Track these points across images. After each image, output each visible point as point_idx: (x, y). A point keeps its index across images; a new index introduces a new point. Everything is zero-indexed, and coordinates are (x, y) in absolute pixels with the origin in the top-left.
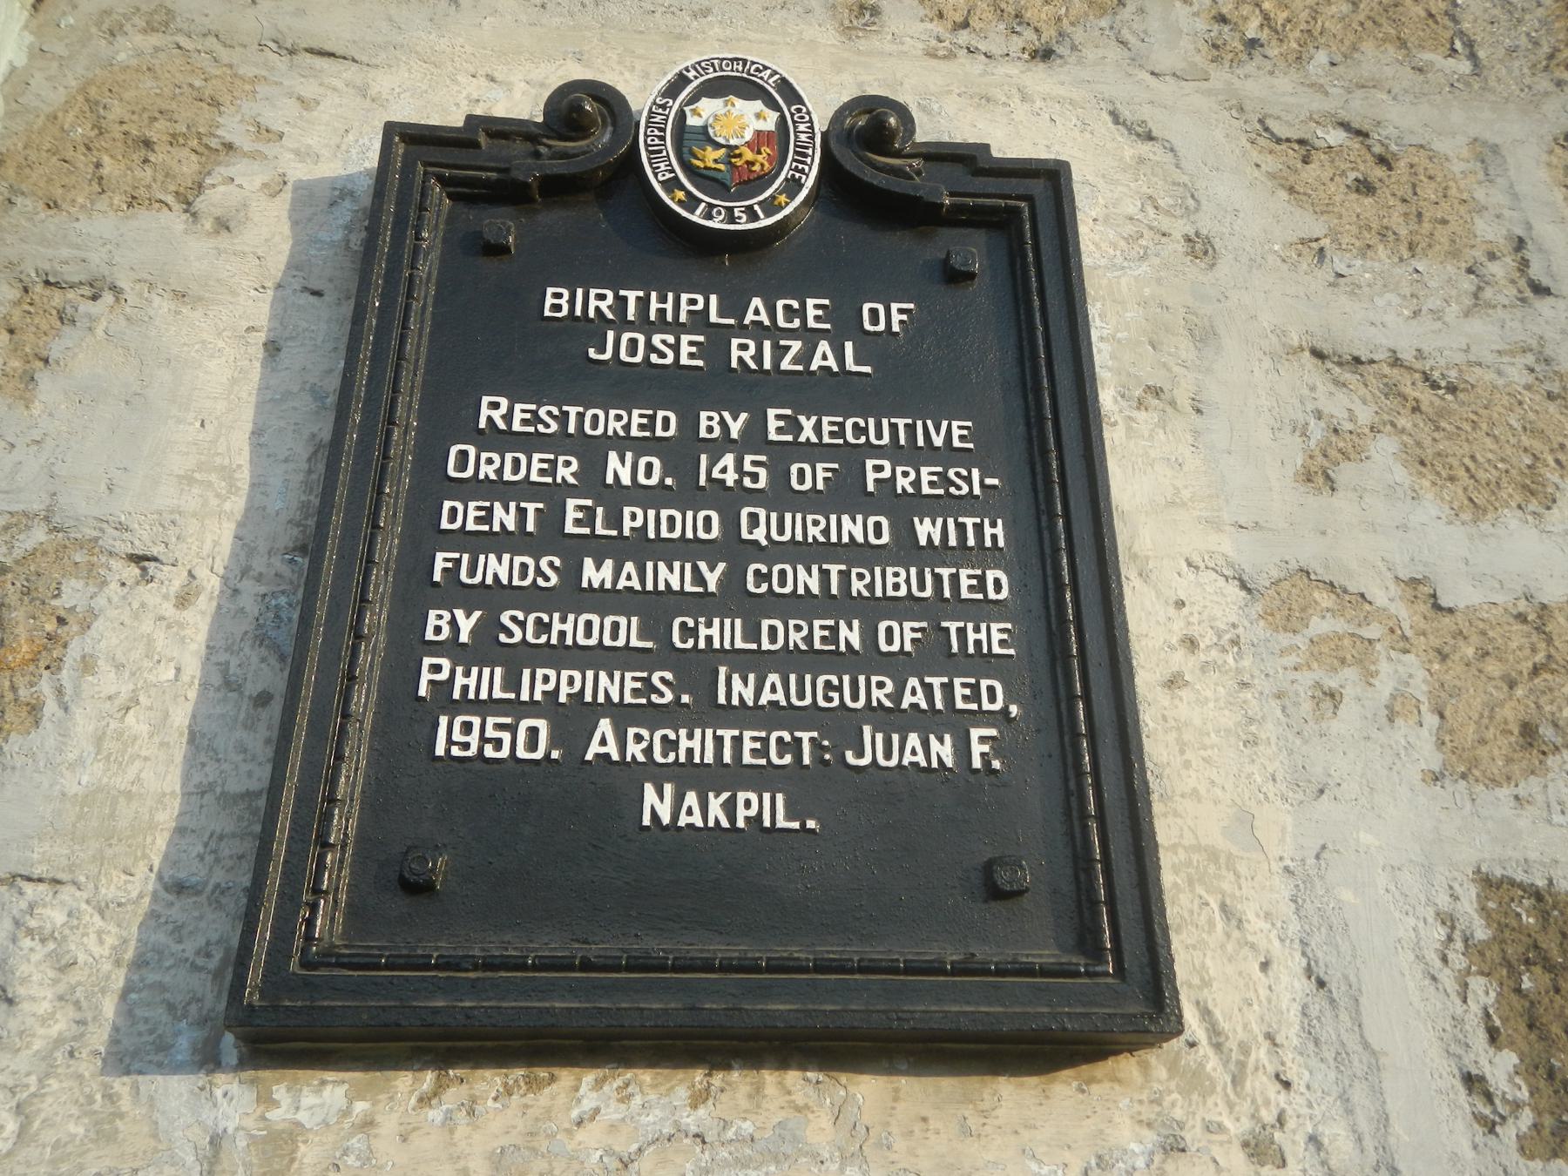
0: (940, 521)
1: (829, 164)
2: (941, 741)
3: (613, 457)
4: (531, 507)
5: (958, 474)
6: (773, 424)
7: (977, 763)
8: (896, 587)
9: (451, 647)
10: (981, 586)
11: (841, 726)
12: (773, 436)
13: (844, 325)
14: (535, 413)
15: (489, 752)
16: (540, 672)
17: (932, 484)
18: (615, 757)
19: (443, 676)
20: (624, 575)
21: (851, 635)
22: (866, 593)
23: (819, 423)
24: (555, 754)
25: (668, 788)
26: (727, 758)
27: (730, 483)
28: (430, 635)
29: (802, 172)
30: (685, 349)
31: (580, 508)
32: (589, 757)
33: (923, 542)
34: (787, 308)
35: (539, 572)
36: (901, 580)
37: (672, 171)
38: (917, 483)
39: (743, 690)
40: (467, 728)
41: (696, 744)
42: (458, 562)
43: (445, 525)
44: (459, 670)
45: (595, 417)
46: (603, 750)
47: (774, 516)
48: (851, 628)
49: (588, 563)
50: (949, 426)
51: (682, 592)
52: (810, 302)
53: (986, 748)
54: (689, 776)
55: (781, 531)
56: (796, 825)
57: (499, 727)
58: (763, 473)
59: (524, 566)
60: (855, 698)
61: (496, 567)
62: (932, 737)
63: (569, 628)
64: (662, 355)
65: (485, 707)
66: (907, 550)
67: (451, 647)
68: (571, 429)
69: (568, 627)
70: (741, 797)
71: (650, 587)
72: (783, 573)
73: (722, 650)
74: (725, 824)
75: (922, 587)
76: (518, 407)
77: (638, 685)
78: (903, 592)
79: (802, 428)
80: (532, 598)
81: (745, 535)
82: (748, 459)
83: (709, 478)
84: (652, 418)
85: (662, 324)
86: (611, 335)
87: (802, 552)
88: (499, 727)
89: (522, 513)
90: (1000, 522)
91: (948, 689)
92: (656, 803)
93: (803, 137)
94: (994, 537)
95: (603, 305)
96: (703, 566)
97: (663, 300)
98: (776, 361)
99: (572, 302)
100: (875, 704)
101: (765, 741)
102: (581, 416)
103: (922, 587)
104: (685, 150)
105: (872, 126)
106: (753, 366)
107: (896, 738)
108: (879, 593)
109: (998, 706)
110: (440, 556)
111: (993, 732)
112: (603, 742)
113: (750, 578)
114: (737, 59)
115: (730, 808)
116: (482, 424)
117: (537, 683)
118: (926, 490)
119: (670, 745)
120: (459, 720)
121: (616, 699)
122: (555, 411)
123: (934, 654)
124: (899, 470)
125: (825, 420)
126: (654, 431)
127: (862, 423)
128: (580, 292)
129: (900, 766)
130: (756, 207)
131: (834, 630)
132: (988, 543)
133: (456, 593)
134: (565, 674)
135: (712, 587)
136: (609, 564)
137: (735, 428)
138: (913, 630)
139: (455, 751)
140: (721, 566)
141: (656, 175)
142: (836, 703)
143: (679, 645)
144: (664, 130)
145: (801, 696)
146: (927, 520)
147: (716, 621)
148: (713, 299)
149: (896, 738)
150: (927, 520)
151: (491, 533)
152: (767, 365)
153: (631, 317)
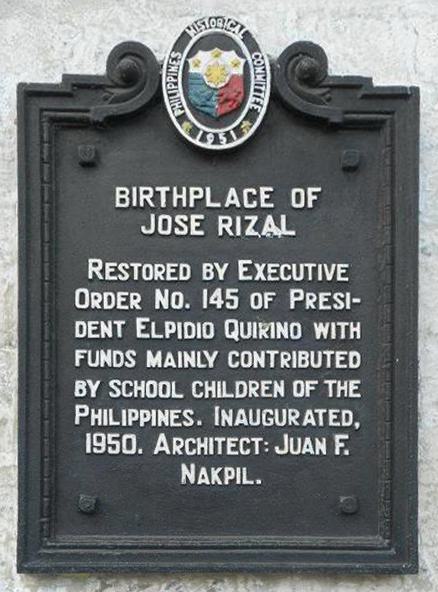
0: (327, 325)
1: (275, 97)
2: (321, 441)
3: (158, 292)
4: (119, 324)
5: (339, 297)
6: (242, 270)
7: (337, 452)
8: (303, 362)
9: (87, 399)
10: (346, 361)
11: (273, 435)
12: (242, 277)
13: (280, 204)
15: (110, 451)
16: (131, 411)
17: (325, 303)
18: (168, 452)
19: (86, 414)
20: (167, 360)
21: (279, 389)
22: (288, 366)
23: (266, 268)
25: (193, 466)
26: (220, 452)
28: (77, 394)
29: (258, 104)
30: (194, 224)
31: (143, 323)
32: (156, 452)
33: (318, 337)
34: (250, 194)
35: (126, 359)
36: (306, 358)
37: (182, 109)
38: (316, 303)
39: (227, 418)
41: (205, 446)
42: (86, 355)
43: (78, 335)
44: (93, 411)
45: (148, 269)
47: (242, 324)
49: (149, 353)
50: (336, 268)
51: (196, 368)
52: (263, 190)
53: (342, 445)
54: (204, 461)
55: (246, 332)
56: (252, 483)
57: (114, 439)
58: (236, 299)
59: (118, 356)
60: (281, 420)
61: (105, 358)
62: (317, 440)
63: (143, 388)
64: (181, 229)
65: (107, 429)
66: (308, 342)
67: (87, 399)
68: (136, 278)
69: (142, 388)
70: (227, 470)
71: (180, 366)
72: (246, 356)
73: (216, 399)
74: (220, 483)
75: (316, 361)
76: (108, 265)
77: (177, 417)
78: (306, 365)
80: (122, 373)
81: (228, 336)
82: (228, 291)
83: (209, 305)
84: (177, 268)
85: (180, 209)
86: (153, 216)
87: (255, 344)
88: (114, 439)
89: (115, 327)
90: (359, 324)
91: (326, 415)
92: (187, 473)
93: (259, 77)
94: (355, 333)
96: (206, 353)
97: (180, 192)
98: (243, 231)
99: (130, 196)
101: (237, 443)
102: (140, 269)
103: (316, 361)
105: (303, 65)
106: (231, 234)
107: (299, 440)
108: (294, 366)
109: (349, 424)
110: (78, 352)
111: (346, 437)
112: (162, 445)
113: (230, 358)
115: (221, 475)
116: (90, 277)
117: (129, 416)
118: (322, 307)
119: (192, 446)
120: (95, 436)
121: (167, 424)
122: (127, 267)
123: (319, 398)
128: (134, 189)
129: (301, 454)
130: (232, 132)
131: (271, 386)
132: (352, 337)
133: (85, 372)
134: (142, 412)
136: (159, 353)
137: (221, 273)
138: (311, 385)
139: (95, 451)
142: (272, 423)
143: (196, 396)
144: (176, 77)
145: (255, 420)
146: (321, 324)
148: (208, 190)
149: (299, 440)
150: (321, 324)
151: (100, 339)
152: (238, 233)
153: (163, 205)
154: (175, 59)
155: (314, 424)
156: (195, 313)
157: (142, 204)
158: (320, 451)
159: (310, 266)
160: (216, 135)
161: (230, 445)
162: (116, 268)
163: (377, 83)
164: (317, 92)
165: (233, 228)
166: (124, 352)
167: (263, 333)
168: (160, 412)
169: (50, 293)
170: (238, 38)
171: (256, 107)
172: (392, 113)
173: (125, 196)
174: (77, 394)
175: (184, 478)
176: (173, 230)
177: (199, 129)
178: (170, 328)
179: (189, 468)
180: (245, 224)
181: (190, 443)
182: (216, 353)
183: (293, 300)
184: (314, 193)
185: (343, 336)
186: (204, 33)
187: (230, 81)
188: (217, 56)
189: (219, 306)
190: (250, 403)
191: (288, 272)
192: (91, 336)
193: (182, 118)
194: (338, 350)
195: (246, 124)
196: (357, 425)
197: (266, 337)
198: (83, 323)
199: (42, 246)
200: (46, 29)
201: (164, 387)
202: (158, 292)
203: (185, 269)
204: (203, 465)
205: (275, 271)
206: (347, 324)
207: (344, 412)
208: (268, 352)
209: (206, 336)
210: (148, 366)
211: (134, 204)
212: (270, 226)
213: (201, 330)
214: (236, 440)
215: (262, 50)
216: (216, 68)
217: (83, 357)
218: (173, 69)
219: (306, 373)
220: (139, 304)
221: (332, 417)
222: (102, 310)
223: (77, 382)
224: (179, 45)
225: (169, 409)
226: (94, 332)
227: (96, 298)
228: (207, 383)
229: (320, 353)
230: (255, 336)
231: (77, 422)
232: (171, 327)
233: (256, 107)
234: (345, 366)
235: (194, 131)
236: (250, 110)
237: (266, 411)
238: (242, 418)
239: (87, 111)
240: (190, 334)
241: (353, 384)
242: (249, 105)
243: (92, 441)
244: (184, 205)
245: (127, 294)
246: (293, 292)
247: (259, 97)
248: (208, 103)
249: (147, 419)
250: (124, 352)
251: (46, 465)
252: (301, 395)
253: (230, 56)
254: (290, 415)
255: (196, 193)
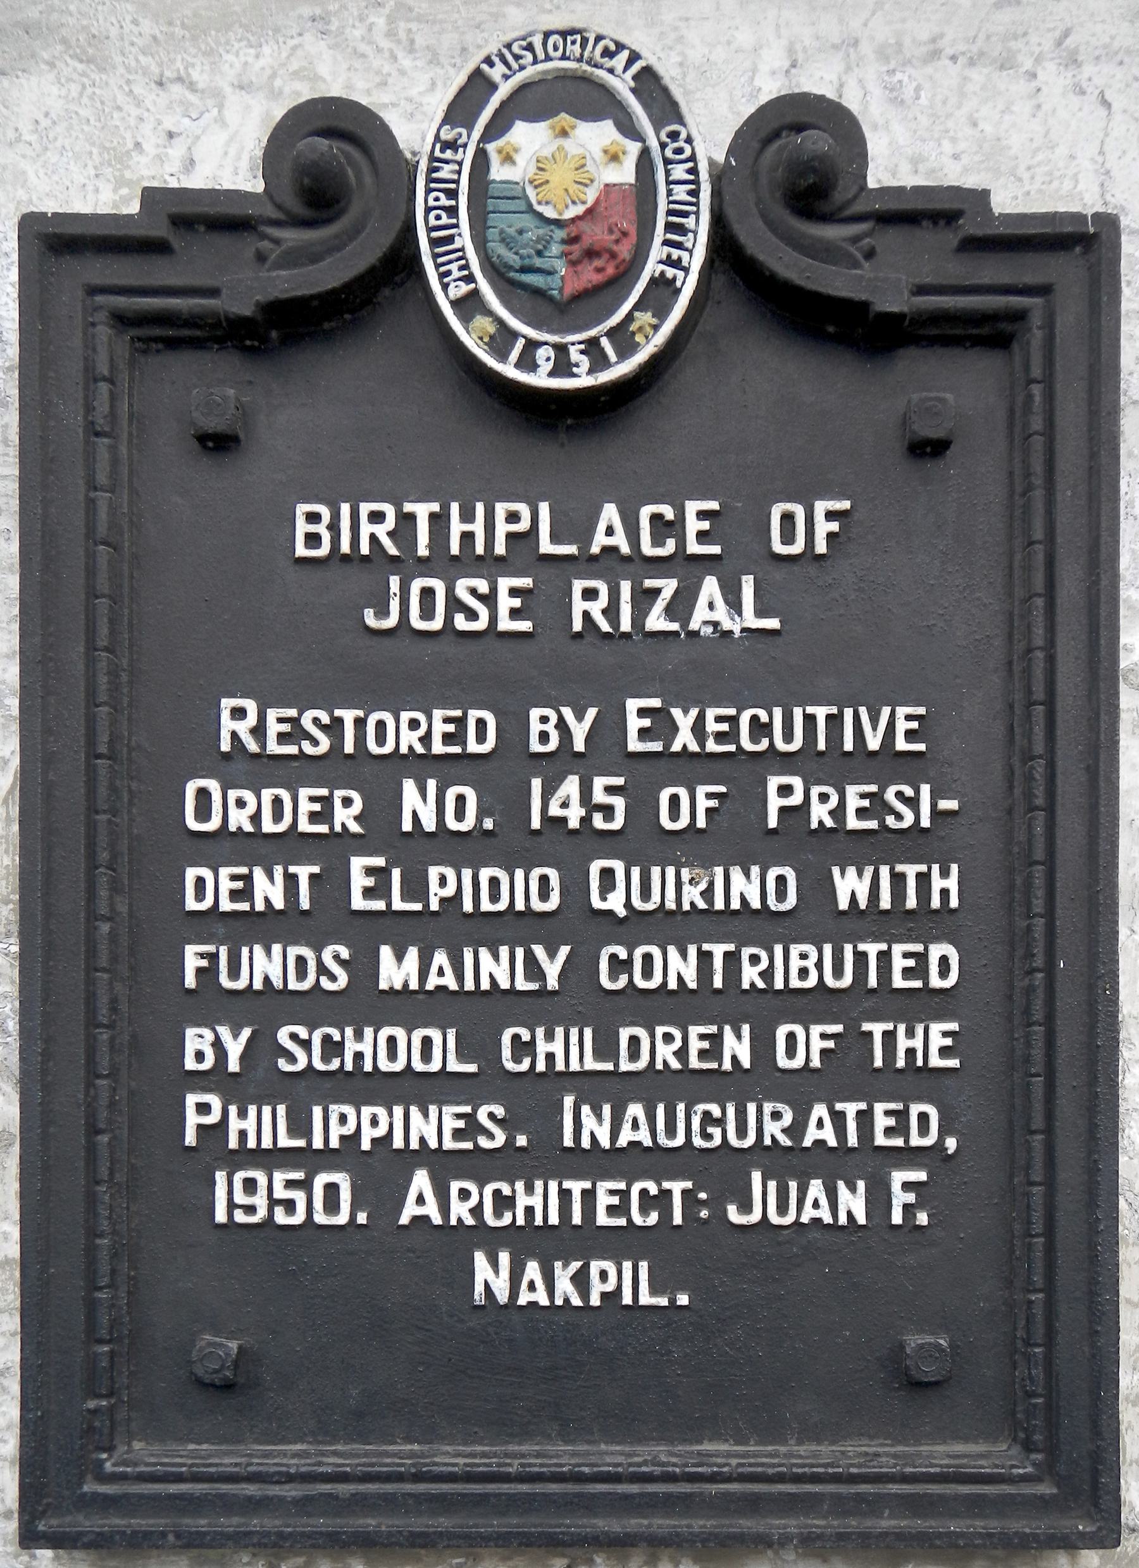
0: (869, 871)
1: (725, 248)
2: (853, 1189)
3: (409, 787)
4: (303, 872)
5: (899, 795)
6: (634, 723)
7: (897, 1218)
8: (803, 973)
10: (919, 969)
11: (722, 1172)
12: (634, 745)
13: (738, 549)
14: (295, 722)
15: (281, 1217)
16: (335, 1109)
17: (861, 813)
18: (437, 1220)
19: (213, 1118)
20: (434, 969)
21: (738, 1047)
22: (761, 985)
23: (701, 718)
24: (362, 1218)
25: (504, 1258)
26: (577, 1220)
27: (574, 824)
28: (190, 1064)
29: (676, 264)
30: (505, 603)
31: (370, 871)
32: (404, 1220)
33: (843, 904)
34: (656, 518)
35: (322, 969)
36: (810, 963)
37: (470, 279)
38: (838, 813)
39: (596, 1128)
40: (250, 1186)
41: (536, 1201)
42: (213, 957)
43: (191, 904)
44: (233, 1110)
45: (381, 725)
46: (420, 1211)
47: (636, 872)
48: (739, 1037)
49: (386, 952)
50: (893, 714)
51: (512, 991)
52: (692, 507)
53: (911, 1198)
54: (533, 1242)
55: (646, 894)
56: (663, 1301)
57: (290, 1184)
58: (619, 803)
59: (301, 961)
60: (742, 1132)
61: (265, 965)
62: (841, 1184)
63: (369, 1047)
64: (472, 615)
66: (817, 918)
67: (216, 1078)
68: (349, 748)
69: (366, 1048)
70: (595, 1266)
71: (469, 985)
72: (648, 958)
73: (567, 1074)
74: (576, 1301)
75: (838, 972)
76: (272, 714)
77: (461, 1124)
78: (812, 981)
79: (676, 729)
80: (313, 1006)
81: (597, 903)
82: (599, 783)
84: (461, 722)
86: (394, 583)
88: (290, 1184)
89: (291, 881)
90: (954, 868)
91: (865, 1119)
92: (490, 1276)
93: (681, 193)
94: (945, 893)
95: (381, 531)
96: (539, 951)
97: (467, 516)
98: (639, 617)
100: (768, 1141)
101: (625, 1195)
102: (360, 723)
103: (838, 972)
104: (492, 234)
105: (800, 156)
106: (605, 627)
107: (793, 1185)
108: (779, 984)
109: (928, 1142)
110: (190, 950)
111: (922, 1176)
112: (420, 1200)
114: (573, 32)
115: (581, 1280)
116: (225, 746)
117: (331, 1124)
118: (853, 823)
119: (503, 1203)
120: (239, 1177)
121: (433, 1144)
122: (325, 719)
123: (847, 1072)
124: (815, 791)
125: (711, 713)
126: (464, 743)
127: (764, 716)
128: (345, 509)
129: (797, 1223)
130: (605, 342)
131: (716, 1040)
132: (936, 903)
133: (212, 1003)
134: (367, 1111)
135: (552, 983)
136: (412, 954)
137: (579, 733)
138: (824, 1036)
139: (240, 1217)
140: (564, 951)
141: (445, 287)
142: (717, 1141)
143: (510, 1066)
144: (452, 194)
145: (671, 1131)
146: (851, 871)
147: (559, 1031)
148: (544, 509)
149: (793, 1185)
150: (851, 871)
151: (252, 913)
152: (626, 625)
153: (423, 551)
154: (451, 145)
155: (832, 1142)
156: (508, 840)
157: (365, 549)
158: (850, 1214)
159: (821, 712)
160: (561, 350)
161: (603, 1200)
162: (295, 722)
163: (1004, 202)
164: (832, 232)
165: (612, 612)
166: (318, 951)
167: (692, 895)
168: (414, 1111)
169: (113, 789)
170: (622, 85)
171: (670, 272)
172: (1044, 290)
173: (321, 529)
174: (190, 1064)
175: (479, 1288)
176: (449, 619)
177: (515, 335)
178: (442, 882)
179: (495, 1264)
180: (644, 598)
181: (497, 1193)
182: (564, 951)
183: (775, 803)
184: (830, 515)
185: (911, 902)
186: (530, 71)
187: (597, 202)
188: (564, 133)
189: (574, 824)
190: (655, 1086)
191: (760, 729)
192: (226, 905)
193: (470, 305)
194: (901, 941)
195: (645, 318)
196: (951, 1144)
197: (702, 905)
198: (206, 873)
199: (91, 662)
200: (121, 99)
201: (427, 1042)
202: (409, 787)
203: (481, 724)
204: (533, 1255)
205: (724, 727)
206: (923, 868)
207: (915, 1109)
208: (706, 947)
209: (537, 905)
210: (383, 985)
211: (345, 547)
212: (711, 606)
213: (526, 889)
214: (622, 1186)
215: (688, 118)
216: (565, 164)
217: (204, 963)
218: (446, 172)
219: (812, 1004)
220: (356, 818)
221: (882, 1122)
222: (258, 835)
223: (190, 1032)
224: (461, 110)
225: (440, 1104)
226: (235, 895)
227: (241, 804)
228: (540, 1032)
229: (848, 949)
230: (671, 905)
231: (190, 1139)
232: (443, 881)
233: (670, 272)
234: (917, 984)
235: (502, 340)
236: (653, 281)
237: (700, 1108)
238: (635, 1125)
239: (214, 292)
240: (495, 897)
241: (938, 1033)
242: (652, 267)
243: (230, 1192)
244: (480, 549)
245: (324, 792)
246: (773, 783)
247: (679, 246)
248: (538, 262)
249: (381, 1131)
250: (318, 951)
251: (104, 1256)
252: (798, 1062)
253: (595, 136)
254: (767, 1118)
255: (513, 517)
